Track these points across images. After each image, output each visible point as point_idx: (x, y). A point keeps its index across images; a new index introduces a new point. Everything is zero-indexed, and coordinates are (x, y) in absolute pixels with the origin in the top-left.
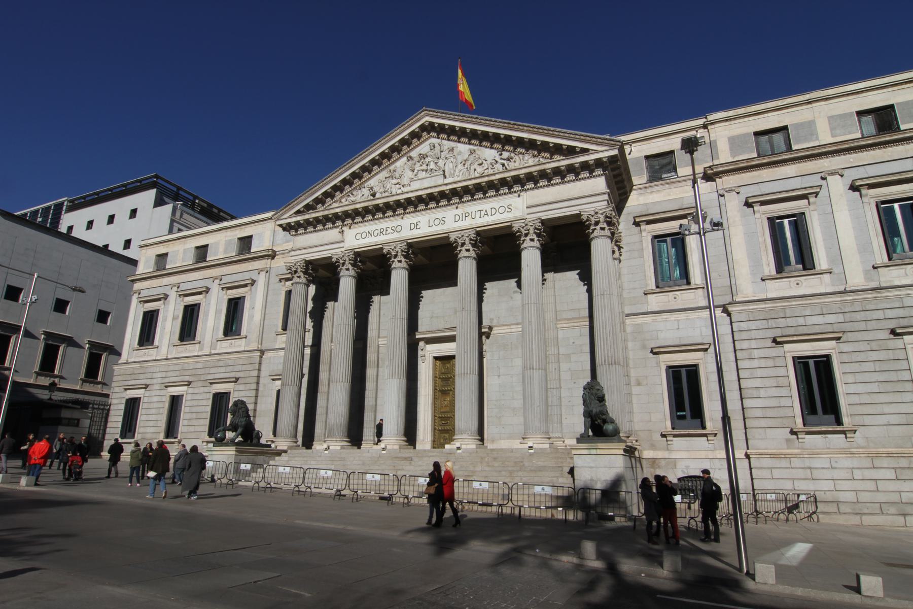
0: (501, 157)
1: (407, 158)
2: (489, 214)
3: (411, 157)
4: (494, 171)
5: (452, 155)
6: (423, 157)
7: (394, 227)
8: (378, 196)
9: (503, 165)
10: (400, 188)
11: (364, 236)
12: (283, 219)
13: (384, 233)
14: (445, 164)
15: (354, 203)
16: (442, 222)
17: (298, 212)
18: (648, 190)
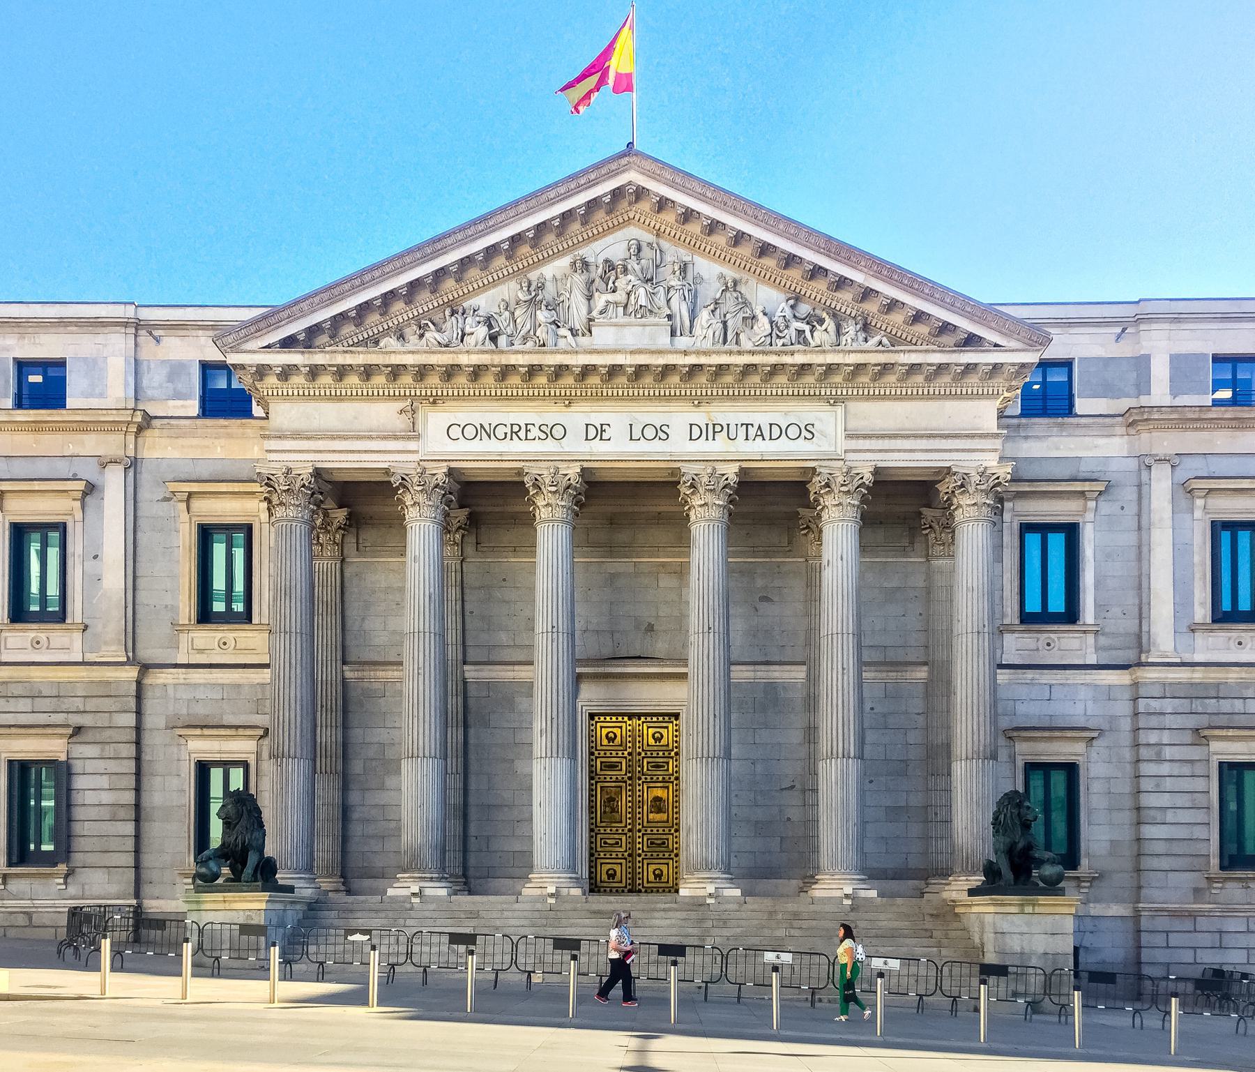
2: (767, 435)
13: (522, 434)
16: (660, 434)
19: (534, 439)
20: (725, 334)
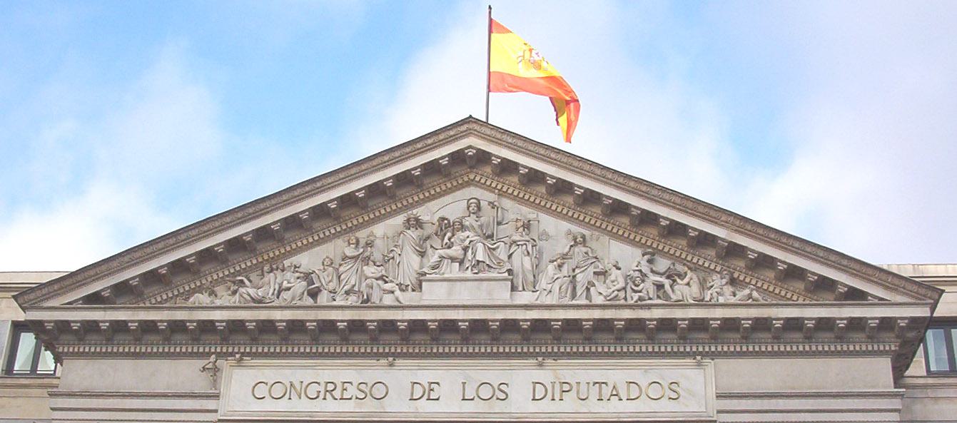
0: (652, 266)
1: (408, 220)
2: (623, 395)
3: (417, 220)
4: (640, 299)
5: (528, 239)
6: (446, 226)
7: (366, 384)
8: (323, 299)
9: (660, 287)
10: (393, 292)
11: (278, 390)
12: (45, 308)
13: (337, 394)
14: (510, 256)
15: (259, 303)
17: (94, 300)
18: (930, 393)
19: (350, 399)
20: (574, 288)
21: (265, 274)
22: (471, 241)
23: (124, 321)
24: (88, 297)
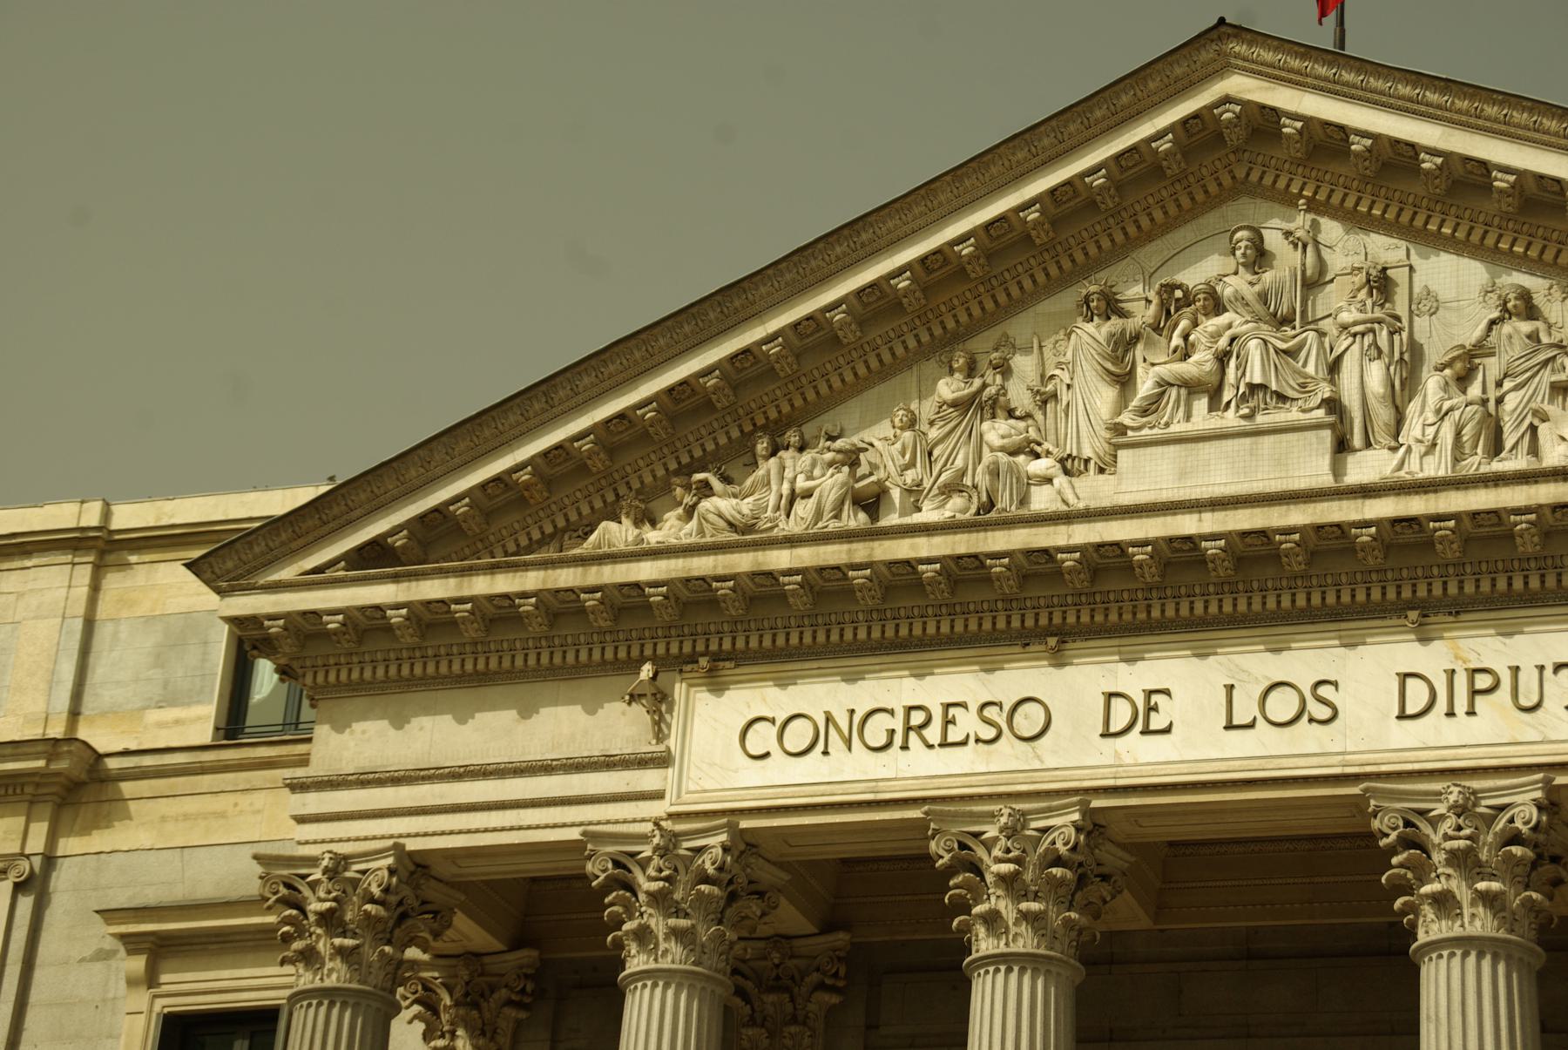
21: (760, 461)
22: (1233, 340)
23: (442, 601)
24: (360, 549)
